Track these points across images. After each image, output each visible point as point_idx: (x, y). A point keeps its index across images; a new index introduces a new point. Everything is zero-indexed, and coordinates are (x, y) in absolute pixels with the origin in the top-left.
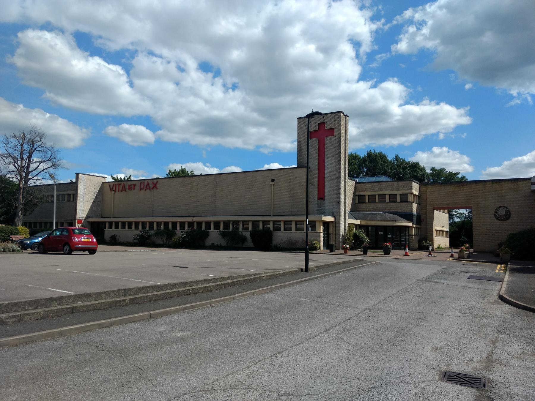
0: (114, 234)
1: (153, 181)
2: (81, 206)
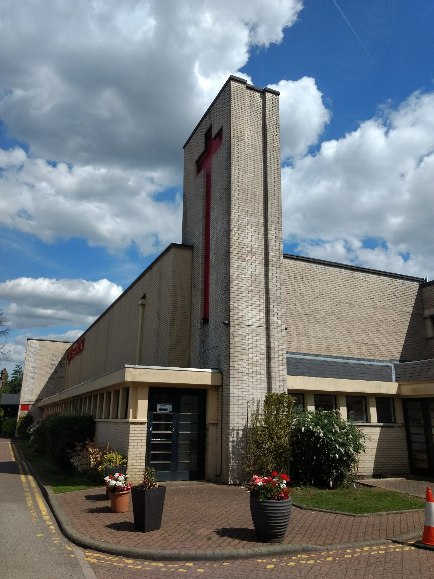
2: (29, 385)
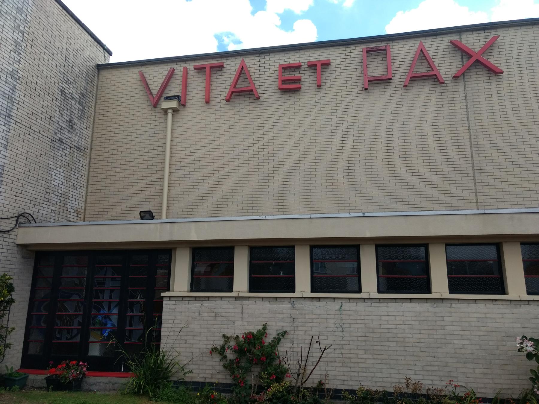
0: (254, 329)
1: (454, 37)
